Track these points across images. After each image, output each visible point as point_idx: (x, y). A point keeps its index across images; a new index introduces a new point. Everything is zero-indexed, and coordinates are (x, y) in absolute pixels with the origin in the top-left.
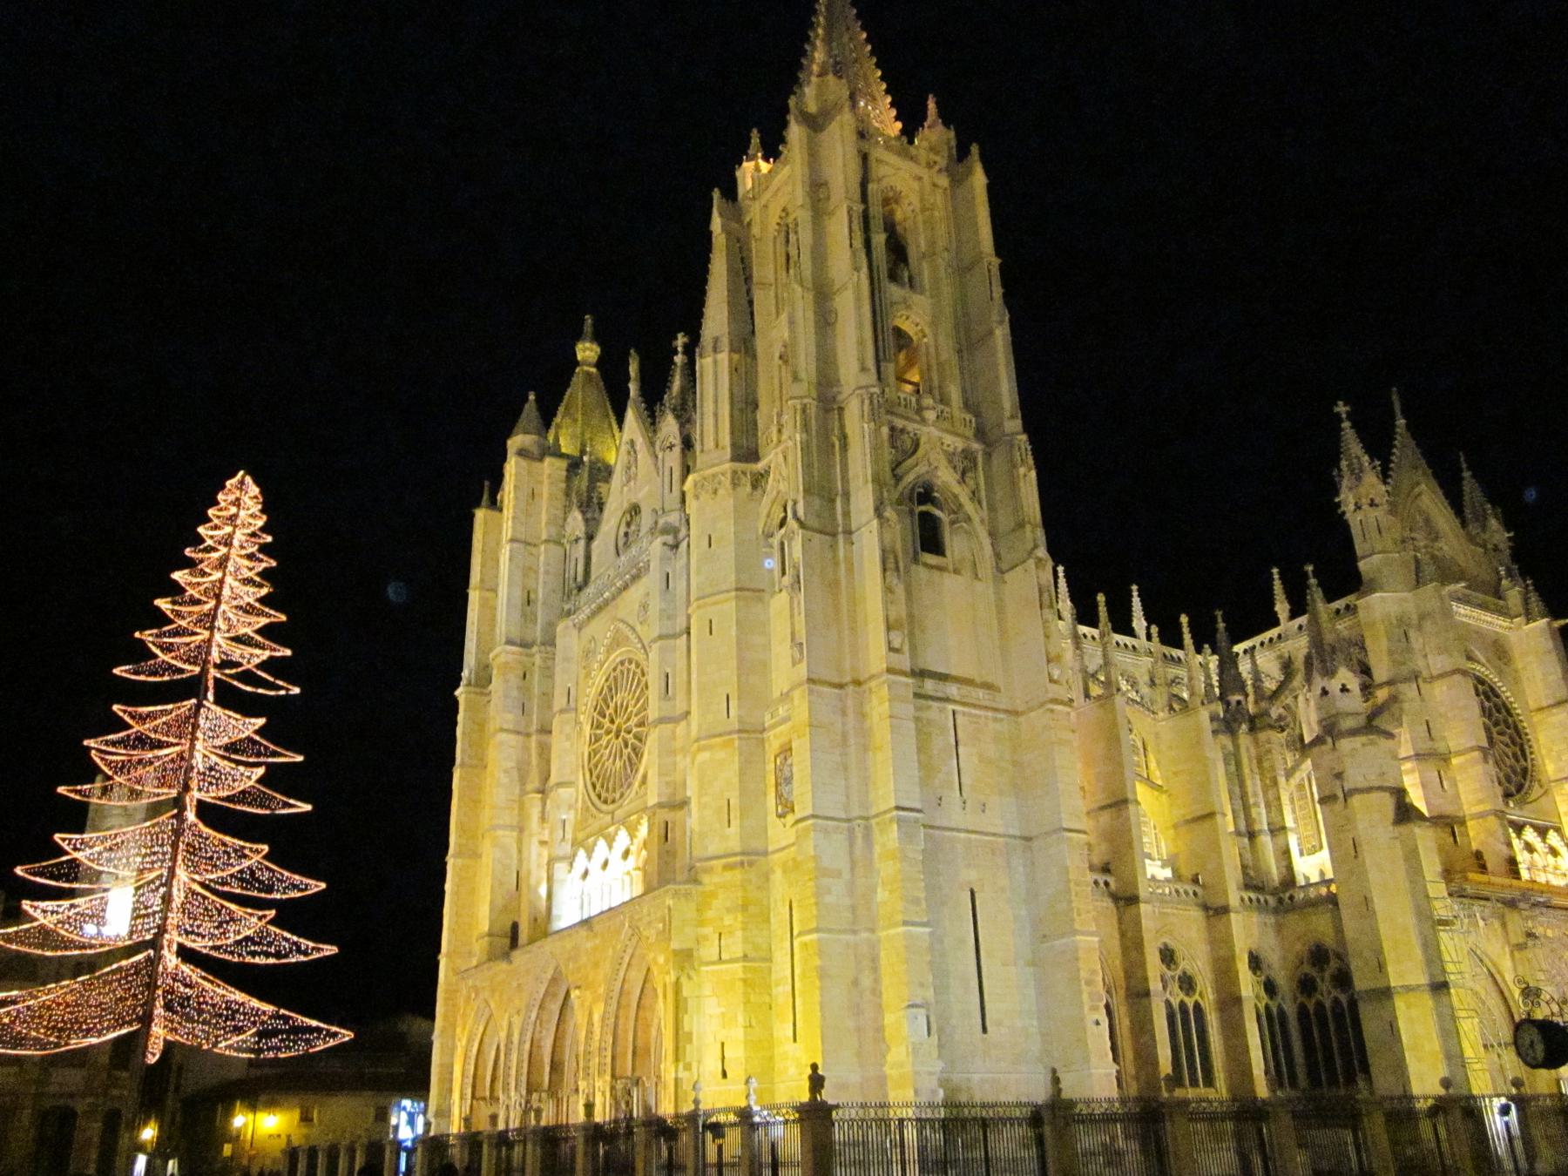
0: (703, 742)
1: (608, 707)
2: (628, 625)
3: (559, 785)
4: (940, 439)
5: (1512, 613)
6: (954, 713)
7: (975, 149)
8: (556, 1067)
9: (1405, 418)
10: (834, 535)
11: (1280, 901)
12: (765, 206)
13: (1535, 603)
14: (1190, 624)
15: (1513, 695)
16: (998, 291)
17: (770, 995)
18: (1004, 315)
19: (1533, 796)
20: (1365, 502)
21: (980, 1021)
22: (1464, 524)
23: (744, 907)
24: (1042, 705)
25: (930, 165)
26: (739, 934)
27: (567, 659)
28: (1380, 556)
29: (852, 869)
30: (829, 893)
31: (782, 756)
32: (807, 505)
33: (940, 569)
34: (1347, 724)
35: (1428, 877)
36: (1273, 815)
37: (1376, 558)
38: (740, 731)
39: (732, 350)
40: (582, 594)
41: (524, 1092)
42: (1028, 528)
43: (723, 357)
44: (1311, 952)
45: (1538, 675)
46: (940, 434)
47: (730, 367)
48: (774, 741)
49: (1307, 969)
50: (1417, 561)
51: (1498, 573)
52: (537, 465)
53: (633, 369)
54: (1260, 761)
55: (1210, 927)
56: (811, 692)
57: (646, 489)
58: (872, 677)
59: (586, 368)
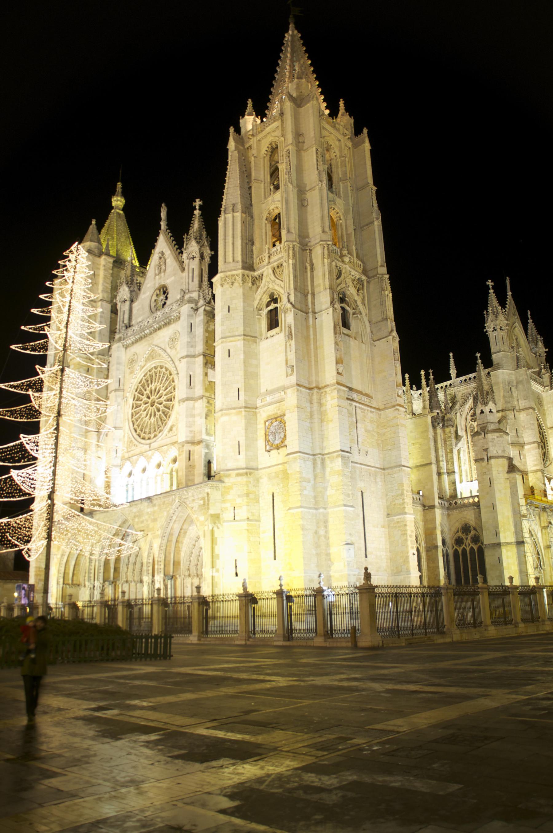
0: (224, 412)
1: (145, 390)
2: (161, 348)
5: (545, 385)
6: (356, 407)
7: (365, 131)
8: (116, 569)
10: (307, 313)
11: (450, 504)
12: (259, 140)
16: (375, 205)
20: (498, 327)
21: (364, 551)
23: (247, 495)
24: (394, 406)
25: (344, 135)
27: (119, 363)
29: (315, 479)
30: (306, 490)
31: (270, 421)
32: (296, 296)
34: (491, 427)
35: (520, 497)
36: (449, 466)
38: (245, 407)
39: (242, 212)
40: (129, 329)
41: (102, 581)
43: (238, 215)
44: (462, 528)
46: (350, 269)
48: (264, 414)
49: (460, 534)
52: (97, 259)
53: (163, 214)
54: (445, 441)
55: (424, 516)
56: (298, 390)
57: (173, 278)
58: (327, 386)
59: (118, 211)
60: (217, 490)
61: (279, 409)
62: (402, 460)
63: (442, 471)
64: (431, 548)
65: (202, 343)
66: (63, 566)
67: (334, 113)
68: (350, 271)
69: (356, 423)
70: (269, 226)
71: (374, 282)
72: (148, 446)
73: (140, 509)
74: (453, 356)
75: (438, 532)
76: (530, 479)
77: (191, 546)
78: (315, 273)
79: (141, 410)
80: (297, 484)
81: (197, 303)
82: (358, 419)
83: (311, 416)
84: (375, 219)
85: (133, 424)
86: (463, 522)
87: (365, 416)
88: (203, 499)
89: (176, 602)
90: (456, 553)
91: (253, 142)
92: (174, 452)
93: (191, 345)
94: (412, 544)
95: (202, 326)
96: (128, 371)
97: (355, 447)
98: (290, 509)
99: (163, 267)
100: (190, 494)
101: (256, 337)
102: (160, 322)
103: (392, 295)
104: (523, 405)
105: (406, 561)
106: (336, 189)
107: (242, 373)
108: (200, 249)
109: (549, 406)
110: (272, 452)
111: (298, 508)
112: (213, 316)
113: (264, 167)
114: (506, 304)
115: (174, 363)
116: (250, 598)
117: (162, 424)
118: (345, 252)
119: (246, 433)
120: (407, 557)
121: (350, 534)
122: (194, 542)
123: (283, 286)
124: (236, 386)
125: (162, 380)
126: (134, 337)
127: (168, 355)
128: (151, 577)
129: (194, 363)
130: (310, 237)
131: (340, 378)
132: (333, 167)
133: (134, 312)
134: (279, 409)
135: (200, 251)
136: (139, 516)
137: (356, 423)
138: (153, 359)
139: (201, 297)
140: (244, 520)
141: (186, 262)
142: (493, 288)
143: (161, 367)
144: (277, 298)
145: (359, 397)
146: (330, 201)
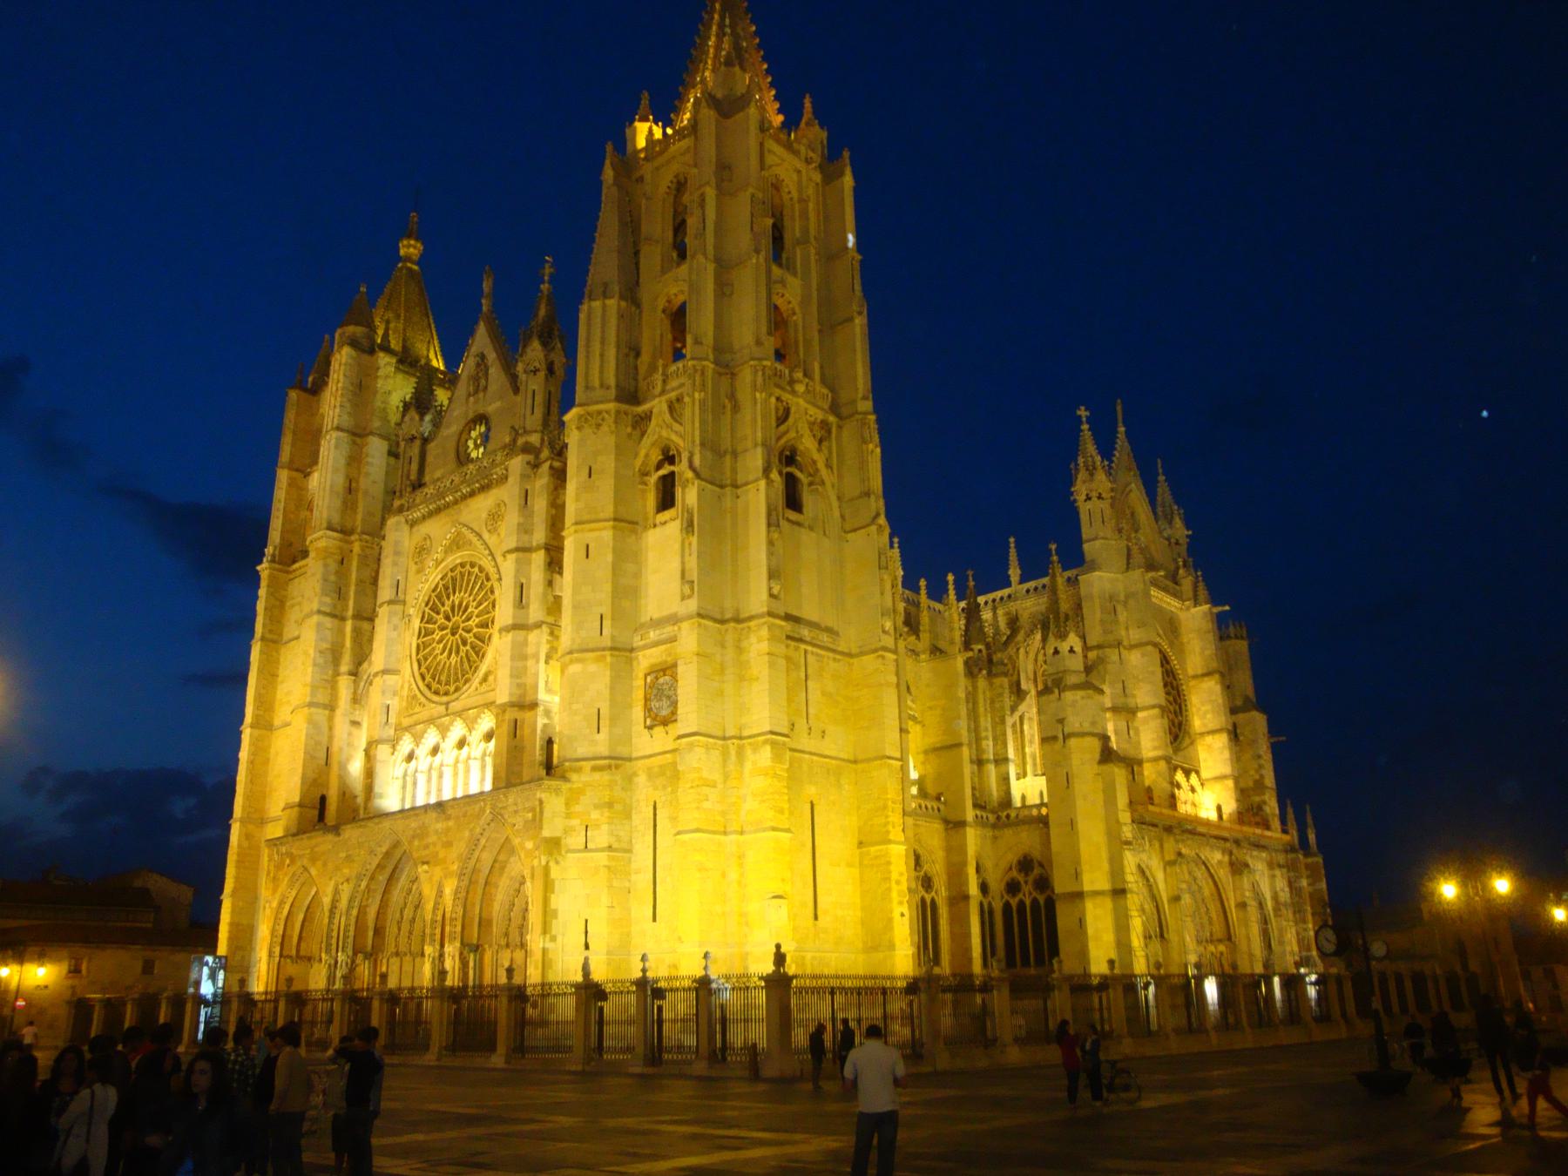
0: (575, 655)
1: (443, 605)
3: (385, 672)
4: (806, 409)
6: (806, 652)
9: (1125, 426)
11: (998, 818)
13: (1203, 593)
14: (955, 582)
15: (1176, 659)
16: (858, 287)
17: (629, 881)
18: (862, 306)
19: (1185, 745)
20: (1094, 494)
22: (1157, 520)
23: (610, 805)
24: (876, 651)
26: (605, 827)
27: (397, 553)
28: (1102, 541)
29: (725, 782)
31: (653, 676)
32: (703, 458)
33: (798, 524)
34: (1072, 679)
36: (999, 747)
37: (1098, 543)
38: (612, 649)
40: (418, 492)
41: (350, 953)
42: (872, 497)
43: (612, 303)
44: (1019, 862)
45: (1197, 649)
46: (806, 405)
47: (618, 313)
48: (646, 660)
49: (1015, 873)
50: (1129, 550)
51: (1177, 563)
52: (366, 357)
53: (487, 286)
54: (992, 702)
56: (700, 625)
57: (498, 404)
58: (751, 618)
59: (409, 265)
60: (557, 795)
61: (670, 655)
63: (985, 757)
64: (959, 899)
65: (544, 525)
66: (282, 923)
68: (806, 409)
69: (806, 680)
70: (667, 323)
72: (443, 707)
75: (971, 871)
76: (1146, 773)
77: (512, 892)
79: (434, 639)
80: (692, 791)
81: (536, 452)
82: (809, 672)
83: (722, 669)
85: (420, 666)
88: (532, 810)
89: (481, 992)
90: (1007, 908)
92: (487, 722)
93: (525, 529)
94: (899, 896)
95: (545, 496)
96: (413, 568)
97: (801, 724)
98: (679, 833)
99: (483, 382)
100: (511, 800)
101: (637, 523)
102: (474, 483)
104: (1137, 637)
106: (788, 259)
107: (608, 587)
108: (545, 356)
109: (1191, 636)
112: (564, 480)
114: (1115, 449)
115: (494, 559)
116: (594, 990)
117: (471, 667)
118: (799, 375)
119: (611, 694)
120: (890, 920)
121: (783, 880)
122: (517, 885)
124: (599, 610)
125: (473, 588)
126: (427, 507)
127: (486, 544)
128: (438, 947)
129: (529, 563)
133: (430, 459)
134: (670, 655)
135: (546, 360)
137: (806, 680)
138: (458, 548)
139: (546, 443)
140: (602, 850)
141: (523, 377)
142: (1088, 422)
143: (473, 565)
144: (673, 456)
145: (812, 635)
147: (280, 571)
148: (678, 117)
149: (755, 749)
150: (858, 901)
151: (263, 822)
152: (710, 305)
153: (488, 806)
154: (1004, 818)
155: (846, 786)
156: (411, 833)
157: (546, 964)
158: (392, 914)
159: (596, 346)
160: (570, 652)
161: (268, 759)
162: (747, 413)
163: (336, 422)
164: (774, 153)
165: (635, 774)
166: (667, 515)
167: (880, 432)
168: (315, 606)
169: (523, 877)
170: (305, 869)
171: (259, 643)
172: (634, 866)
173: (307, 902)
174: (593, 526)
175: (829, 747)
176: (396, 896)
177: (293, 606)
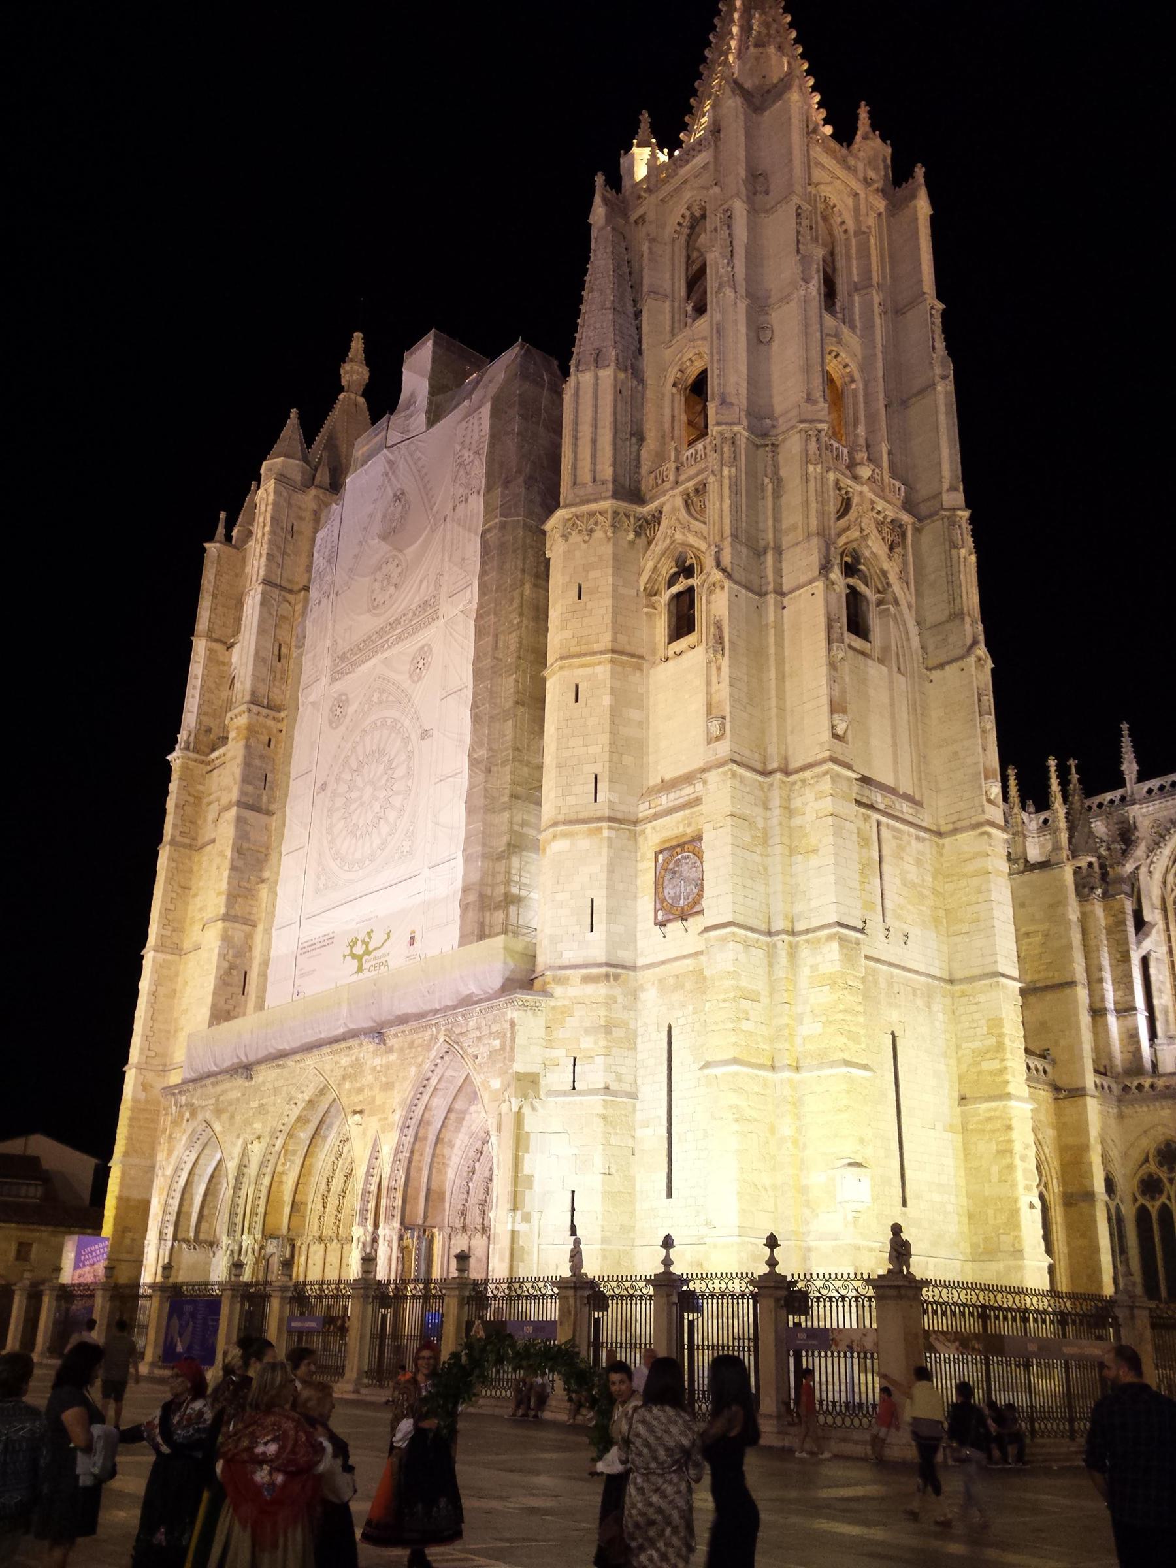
6: (879, 823)
7: (920, 171)
11: (1126, 1089)
16: (940, 345)
23: (608, 1029)
24: (979, 825)
25: (867, 182)
26: (599, 1060)
29: (771, 995)
32: (736, 554)
38: (611, 819)
41: (259, 1236)
42: (968, 620)
43: (607, 374)
44: (1159, 1152)
49: (1152, 1167)
55: (1059, 1113)
61: (689, 825)
62: (999, 958)
66: (178, 1195)
67: (844, 134)
68: (872, 502)
69: (880, 862)
70: (680, 400)
71: (932, 529)
73: (357, 1059)
74: (1129, 729)
75: (1095, 1158)
77: (472, 1154)
78: (784, 500)
82: (884, 852)
83: (765, 839)
84: (937, 378)
86: (1161, 1138)
87: (901, 848)
88: (500, 1035)
90: (1143, 1215)
91: (648, 206)
98: (707, 1065)
101: (642, 658)
103: (978, 558)
105: (1013, 1221)
106: (843, 309)
107: (605, 739)
110: (670, 926)
111: (726, 1063)
113: (673, 264)
118: (862, 455)
119: (608, 879)
120: (1014, 1213)
121: (862, 1141)
123: (705, 534)
128: (370, 1228)
130: (776, 415)
131: (839, 749)
132: (838, 258)
136: (353, 1077)
137: (880, 862)
144: (692, 566)
145: (887, 801)
146: (828, 335)
147: (196, 761)
148: (694, 120)
149: (815, 944)
150: (962, 1182)
151: (164, 1070)
152: (743, 354)
153: (442, 1033)
154: (1133, 1088)
155: (940, 1015)
156: (341, 1072)
157: (514, 1254)
158: (316, 1182)
159: (586, 431)
160: (555, 824)
161: (175, 991)
162: (793, 497)
163: (262, 573)
164: (823, 167)
165: (642, 988)
166: (683, 643)
167: (975, 534)
168: (234, 795)
169: (487, 1133)
170: (209, 1124)
171: (168, 847)
172: (639, 1116)
173: (210, 1170)
174: (584, 660)
175: (914, 956)
176: (323, 1159)
177: (209, 804)
